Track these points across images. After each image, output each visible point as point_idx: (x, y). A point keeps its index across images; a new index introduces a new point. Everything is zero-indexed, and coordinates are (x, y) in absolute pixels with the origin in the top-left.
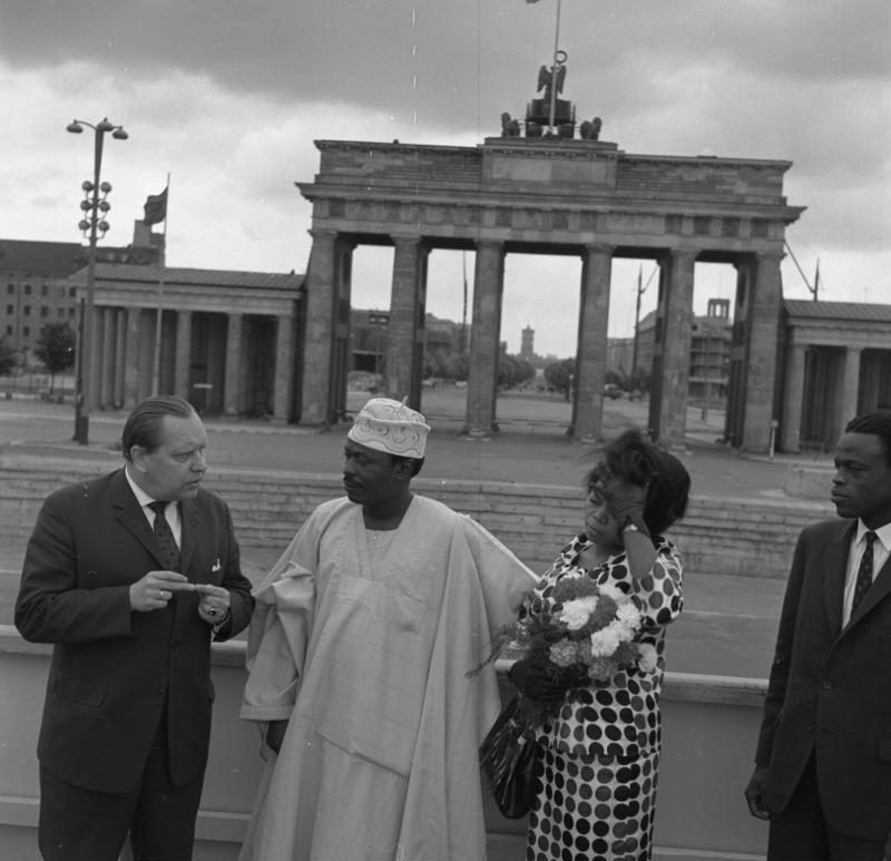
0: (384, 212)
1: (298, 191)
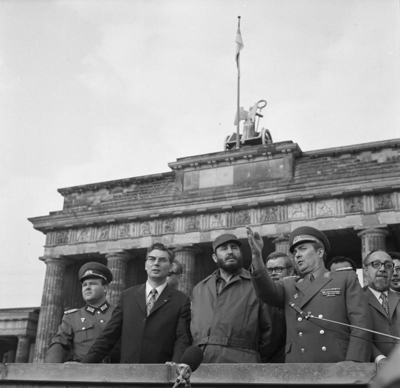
0: (98, 233)
1: (31, 225)
